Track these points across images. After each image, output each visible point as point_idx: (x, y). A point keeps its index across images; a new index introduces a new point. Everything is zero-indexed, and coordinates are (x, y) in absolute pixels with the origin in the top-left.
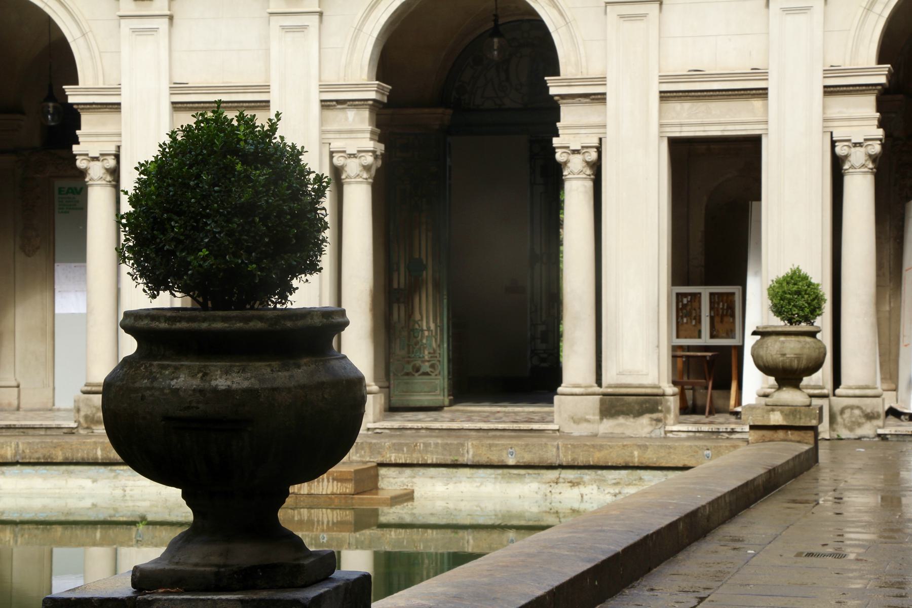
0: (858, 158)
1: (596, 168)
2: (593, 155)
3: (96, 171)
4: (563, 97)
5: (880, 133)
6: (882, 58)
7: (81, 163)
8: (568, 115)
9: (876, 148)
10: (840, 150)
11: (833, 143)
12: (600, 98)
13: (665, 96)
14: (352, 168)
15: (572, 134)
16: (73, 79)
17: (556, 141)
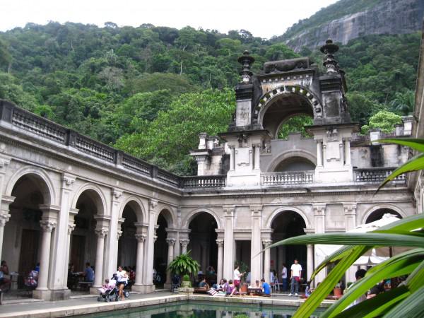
3: (220, 244)
14: (267, 245)
16: (217, 228)
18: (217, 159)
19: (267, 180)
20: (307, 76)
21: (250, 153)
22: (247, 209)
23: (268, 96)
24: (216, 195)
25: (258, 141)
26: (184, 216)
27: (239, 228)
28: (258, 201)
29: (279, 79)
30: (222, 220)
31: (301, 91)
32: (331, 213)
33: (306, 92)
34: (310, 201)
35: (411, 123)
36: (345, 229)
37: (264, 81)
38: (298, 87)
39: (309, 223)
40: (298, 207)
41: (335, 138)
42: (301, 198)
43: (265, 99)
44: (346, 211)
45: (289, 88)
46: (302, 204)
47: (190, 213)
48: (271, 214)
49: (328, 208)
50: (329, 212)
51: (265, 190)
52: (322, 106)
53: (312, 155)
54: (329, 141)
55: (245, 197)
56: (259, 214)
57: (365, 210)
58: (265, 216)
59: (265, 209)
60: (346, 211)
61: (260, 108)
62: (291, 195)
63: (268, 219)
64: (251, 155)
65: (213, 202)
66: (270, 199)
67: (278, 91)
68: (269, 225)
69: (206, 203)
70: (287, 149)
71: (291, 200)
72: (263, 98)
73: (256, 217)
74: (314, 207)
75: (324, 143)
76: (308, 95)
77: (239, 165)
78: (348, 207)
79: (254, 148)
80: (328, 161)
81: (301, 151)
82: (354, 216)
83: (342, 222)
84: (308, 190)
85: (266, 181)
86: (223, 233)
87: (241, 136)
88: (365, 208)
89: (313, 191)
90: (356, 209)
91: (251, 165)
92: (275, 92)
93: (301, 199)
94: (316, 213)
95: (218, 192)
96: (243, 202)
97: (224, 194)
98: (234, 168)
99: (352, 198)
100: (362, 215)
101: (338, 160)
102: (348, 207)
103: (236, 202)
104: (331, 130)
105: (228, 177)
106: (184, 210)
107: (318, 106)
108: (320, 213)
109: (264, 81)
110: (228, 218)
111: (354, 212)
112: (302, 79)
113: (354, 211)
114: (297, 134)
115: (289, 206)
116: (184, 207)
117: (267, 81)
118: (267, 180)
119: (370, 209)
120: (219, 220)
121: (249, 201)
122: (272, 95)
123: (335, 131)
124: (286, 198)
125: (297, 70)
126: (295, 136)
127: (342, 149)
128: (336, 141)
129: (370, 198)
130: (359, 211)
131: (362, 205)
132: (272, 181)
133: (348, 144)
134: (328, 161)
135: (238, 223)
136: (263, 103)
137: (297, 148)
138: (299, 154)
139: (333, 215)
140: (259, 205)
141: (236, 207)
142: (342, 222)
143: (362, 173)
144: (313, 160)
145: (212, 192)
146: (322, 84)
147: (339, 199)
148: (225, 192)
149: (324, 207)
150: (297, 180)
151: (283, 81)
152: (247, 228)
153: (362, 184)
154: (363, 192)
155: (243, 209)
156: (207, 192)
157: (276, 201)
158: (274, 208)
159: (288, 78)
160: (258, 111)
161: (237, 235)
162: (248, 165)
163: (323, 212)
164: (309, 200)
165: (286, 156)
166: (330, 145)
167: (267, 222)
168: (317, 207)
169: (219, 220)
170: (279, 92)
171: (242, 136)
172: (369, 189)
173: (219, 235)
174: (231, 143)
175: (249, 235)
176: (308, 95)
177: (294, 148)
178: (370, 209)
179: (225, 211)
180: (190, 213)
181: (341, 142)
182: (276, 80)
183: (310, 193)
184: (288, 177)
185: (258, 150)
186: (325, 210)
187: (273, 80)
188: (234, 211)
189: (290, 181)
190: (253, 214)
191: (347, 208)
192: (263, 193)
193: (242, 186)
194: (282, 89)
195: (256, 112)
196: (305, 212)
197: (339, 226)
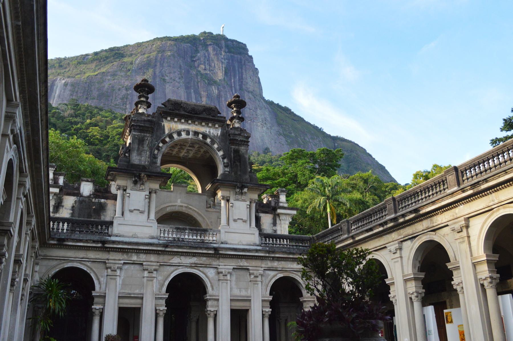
0: (267, 315)
1: (216, 315)
2: (215, 313)
3: (97, 312)
4: (210, 299)
5: (271, 310)
6: (270, 294)
7: (94, 310)
8: (209, 303)
9: (270, 313)
10: (264, 313)
11: (262, 311)
12: (218, 300)
13: (231, 300)
14: (161, 313)
15: (211, 307)
16: (94, 290)
17: (208, 309)
18: (69, 201)
19: (164, 234)
20: (217, 126)
21: (146, 198)
22: (137, 267)
23: (171, 136)
24: (100, 245)
25: (156, 186)
26: (44, 270)
27: (127, 291)
28: (153, 258)
29: (187, 121)
30: (102, 279)
31: (208, 140)
32: (237, 278)
33: (213, 142)
34: (214, 263)
35: (285, 196)
36: (250, 297)
37: (169, 119)
38: (205, 136)
39: (213, 289)
40: (201, 269)
41: (244, 197)
42: (204, 258)
43: (167, 139)
44: (252, 276)
45: (196, 133)
46: (206, 266)
47: (55, 267)
48: (169, 275)
49: (234, 273)
50: (234, 278)
51: (166, 246)
52: (231, 162)
53: (198, 213)
54: (237, 200)
55: (138, 252)
56: (155, 274)
57: (270, 277)
58: (160, 278)
59: (162, 268)
60: (252, 276)
61: (161, 148)
62: (194, 255)
63: (164, 282)
64: (147, 200)
65: (92, 255)
66: (170, 257)
67: (183, 133)
68: (164, 289)
69: (81, 254)
70: (171, 202)
71: (194, 260)
72: (165, 138)
73: (150, 279)
74: (219, 270)
75: (232, 201)
76: (216, 146)
77: (131, 211)
78: (255, 272)
79: (150, 193)
80: (235, 221)
81: (186, 207)
82: (260, 283)
83: (246, 289)
84: (215, 249)
85: (162, 235)
86: (104, 297)
87: (139, 177)
88: (269, 275)
89: (221, 252)
90: (262, 275)
91: (146, 214)
92: (179, 133)
93: (204, 260)
94: (222, 277)
95: (104, 242)
96: (134, 258)
97: (111, 246)
98: (123, 214)
99: (257, 263)
100: (267, 281)
101: (245, 221)
102: (255, 272)
103: (125, 256)
104: (242, 187)
105: (115, 224)
106: (45, 262)
107: (226, 161)
108: (225, 277)
109: (169, 119)
110: (113, 277)
111: (259, 279)
112: (210, 127)
113: (260, 277)
114: (183, 186)
115: (191, 267)
116: (46, 258)
117: (172, 119)
118: (164, 234)
119: (274, 276)
120: (98, 279)
121: (143, 257)
122: (175, 136)
123: (246, 190)
124: (188, 258)
125: (204, 115)
126: (181, 188)
127: (249, 209)
128: (244, 201)
129: (276, 264)
130: (264, 278)
131: (267, 272)
132: (170, 235)
133: (254, 205)
134: (235, 221)
135: (124, 285)
136: (164, 142)
137: (181, 202)
138: (184, 210)
139: (238, 280)
140: (155, 264)
141: (124, 263)
142: (246, 289)
143: (265, 238)
144: (199, 219)
145: (94, 242)
146: (232, 138)
147: (244, 263)
148: (114, 242)
149: (231, 270)
150: (199, 238)
151: (190, 124)
152: (137, 291)
153: (268, 248)
154: (271, 257)
155: (132, 266)
156: (87, 241)
157: (176, 260)
158: (172, 268)
159: (197, 123)
160: (159, 150)
161: (121, 301)
162: (142, 212)
163: (229, 276)
164: (215, 263)
165: (169, 210)
166: (237, 204)
167: (163, 285)
168: (223, 270)
169: (98, 279)
170: (184, 135)
171: (138, 175)
172: (277, 255)
173: (96, 300)
174: (120, 182)
175: (139, 301)
176: (216, 146)
177: (179, 202)
178: (274, 276)
179: (107, 268)
180: (55, 267)
181: (248, 203)
182: (183, 121)
183: (217, 253)
184: (189, 233)
185: (154, 195)
186: (230, 273)
187: (179, 120)
188: (121, 269)
189: (188, 236)
190: (146, 274)
191: (253, 274)
192: (163, 249)
193: (132, 237)
194: (188, 133)
195: (156, 152)
196: (208, 275)
197: (244, 293)
